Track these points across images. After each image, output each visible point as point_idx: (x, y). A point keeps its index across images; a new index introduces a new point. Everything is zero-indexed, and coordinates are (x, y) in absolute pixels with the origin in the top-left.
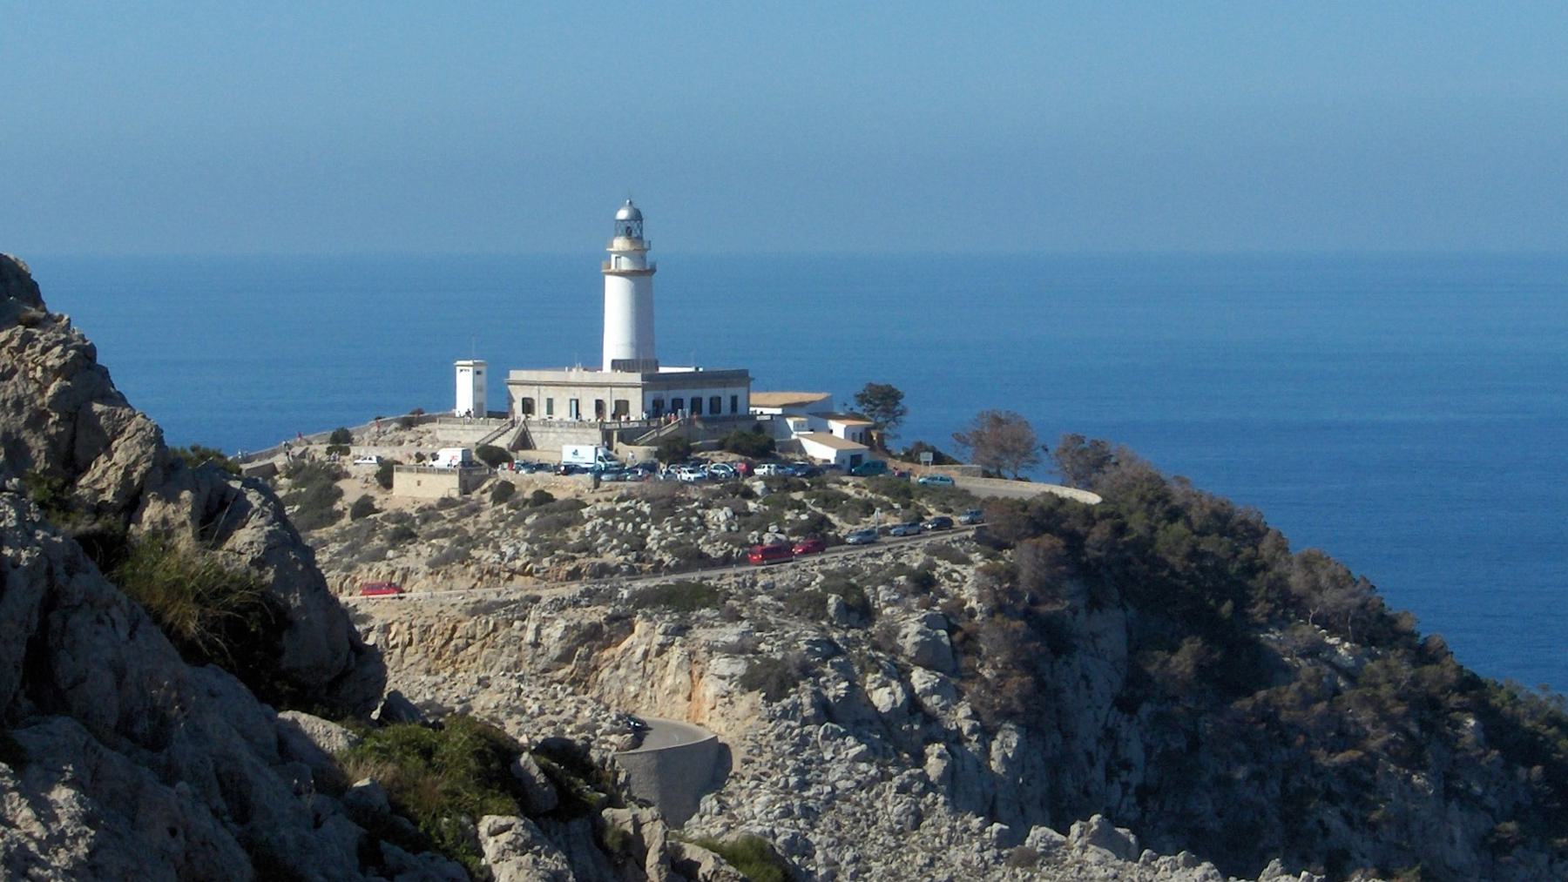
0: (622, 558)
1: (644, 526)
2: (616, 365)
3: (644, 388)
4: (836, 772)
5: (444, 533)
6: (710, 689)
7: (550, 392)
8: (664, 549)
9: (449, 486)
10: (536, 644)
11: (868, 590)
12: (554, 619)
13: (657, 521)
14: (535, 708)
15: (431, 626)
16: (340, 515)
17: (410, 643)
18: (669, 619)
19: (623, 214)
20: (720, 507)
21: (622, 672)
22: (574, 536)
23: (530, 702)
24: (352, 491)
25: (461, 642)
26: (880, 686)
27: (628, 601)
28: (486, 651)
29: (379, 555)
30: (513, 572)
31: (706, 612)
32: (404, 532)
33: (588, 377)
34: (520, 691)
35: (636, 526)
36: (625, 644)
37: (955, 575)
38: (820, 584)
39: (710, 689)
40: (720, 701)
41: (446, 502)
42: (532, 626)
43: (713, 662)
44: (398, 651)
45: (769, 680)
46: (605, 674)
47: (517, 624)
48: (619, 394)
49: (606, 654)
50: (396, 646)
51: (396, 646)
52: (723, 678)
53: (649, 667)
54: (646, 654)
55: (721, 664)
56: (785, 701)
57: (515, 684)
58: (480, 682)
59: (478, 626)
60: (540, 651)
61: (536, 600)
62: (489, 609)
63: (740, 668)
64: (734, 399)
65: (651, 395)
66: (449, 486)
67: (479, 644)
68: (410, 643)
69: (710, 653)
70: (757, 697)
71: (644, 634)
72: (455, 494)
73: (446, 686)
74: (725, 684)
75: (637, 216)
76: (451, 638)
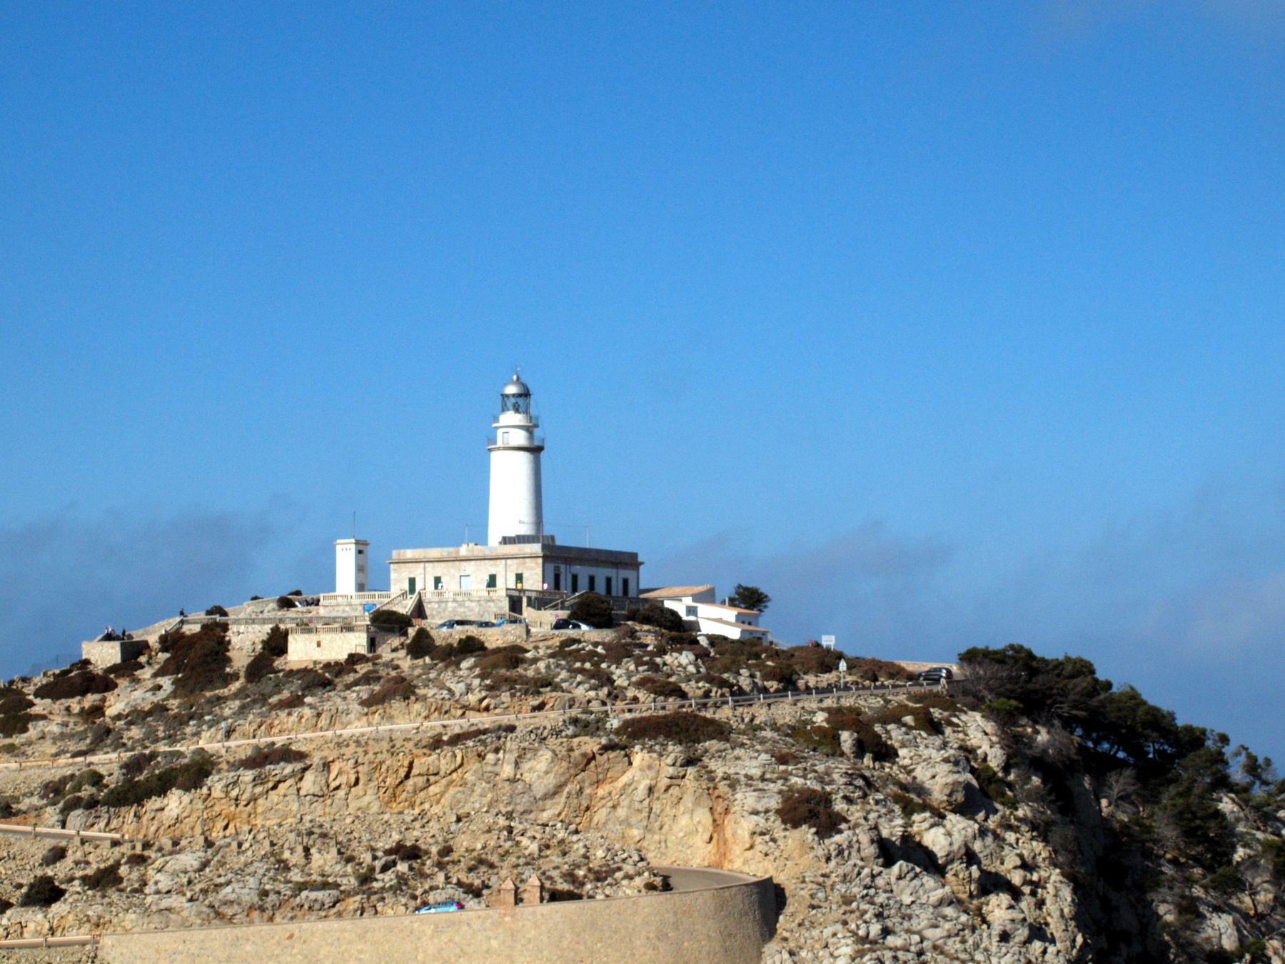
0: (592, 694)
1: (604, 666)
2: (506, 541)
3: (546, 559)
4: (922, 919)
6: (741, 827)
7: (439, 570)
9: (357, 642)
10: (512, 781)
12: (536, 750)
14: (534, 848)
15: (381, 763)
17: (357, 782)
18: (675, 751)
19: (512, 390)
20: (680, 651)
21: (622, 812)
23: (525, 841)
25: (421, 781)
26: (932, 826)
27: (617, 732)
28: (452, 791)
30: (466, 708)
31: (713, 745)
32: (320, 679)
33: (479, 550)
34: (510, 830)
35: (596, 665)
36: (625, 779)
37: (955, 720)
38: (827, 720)
39: (741, 827)
40: (758, 839)
41: (354, 659)
42: (511, 757)
43: (739, 796)
44: (341, 793)
45: (810, 812)
46: (601, 815)
47: (491, 757)
49: (601, 792)
50: (337, 788)
51: (337, 788)
52: (756, 813)
53: (657, 807)
54: (651, 790)
55: (746, 798)
56: (837, 838)
57: (502, 821)
58: (459, 820)
59: (443, 760)
60: (520, 786)
61: (511, 729)
62: (456, 740)
63: (774, 803)
64: (626, 582)
65: (550, 567)
66: (357, 642)
67: (444, 782)
68: (357, 782)
71: (645, 766)
72: (363, 650)
73: (417, 824)
74: (760, 819)
75: (525, 394)
76: (407, 776)
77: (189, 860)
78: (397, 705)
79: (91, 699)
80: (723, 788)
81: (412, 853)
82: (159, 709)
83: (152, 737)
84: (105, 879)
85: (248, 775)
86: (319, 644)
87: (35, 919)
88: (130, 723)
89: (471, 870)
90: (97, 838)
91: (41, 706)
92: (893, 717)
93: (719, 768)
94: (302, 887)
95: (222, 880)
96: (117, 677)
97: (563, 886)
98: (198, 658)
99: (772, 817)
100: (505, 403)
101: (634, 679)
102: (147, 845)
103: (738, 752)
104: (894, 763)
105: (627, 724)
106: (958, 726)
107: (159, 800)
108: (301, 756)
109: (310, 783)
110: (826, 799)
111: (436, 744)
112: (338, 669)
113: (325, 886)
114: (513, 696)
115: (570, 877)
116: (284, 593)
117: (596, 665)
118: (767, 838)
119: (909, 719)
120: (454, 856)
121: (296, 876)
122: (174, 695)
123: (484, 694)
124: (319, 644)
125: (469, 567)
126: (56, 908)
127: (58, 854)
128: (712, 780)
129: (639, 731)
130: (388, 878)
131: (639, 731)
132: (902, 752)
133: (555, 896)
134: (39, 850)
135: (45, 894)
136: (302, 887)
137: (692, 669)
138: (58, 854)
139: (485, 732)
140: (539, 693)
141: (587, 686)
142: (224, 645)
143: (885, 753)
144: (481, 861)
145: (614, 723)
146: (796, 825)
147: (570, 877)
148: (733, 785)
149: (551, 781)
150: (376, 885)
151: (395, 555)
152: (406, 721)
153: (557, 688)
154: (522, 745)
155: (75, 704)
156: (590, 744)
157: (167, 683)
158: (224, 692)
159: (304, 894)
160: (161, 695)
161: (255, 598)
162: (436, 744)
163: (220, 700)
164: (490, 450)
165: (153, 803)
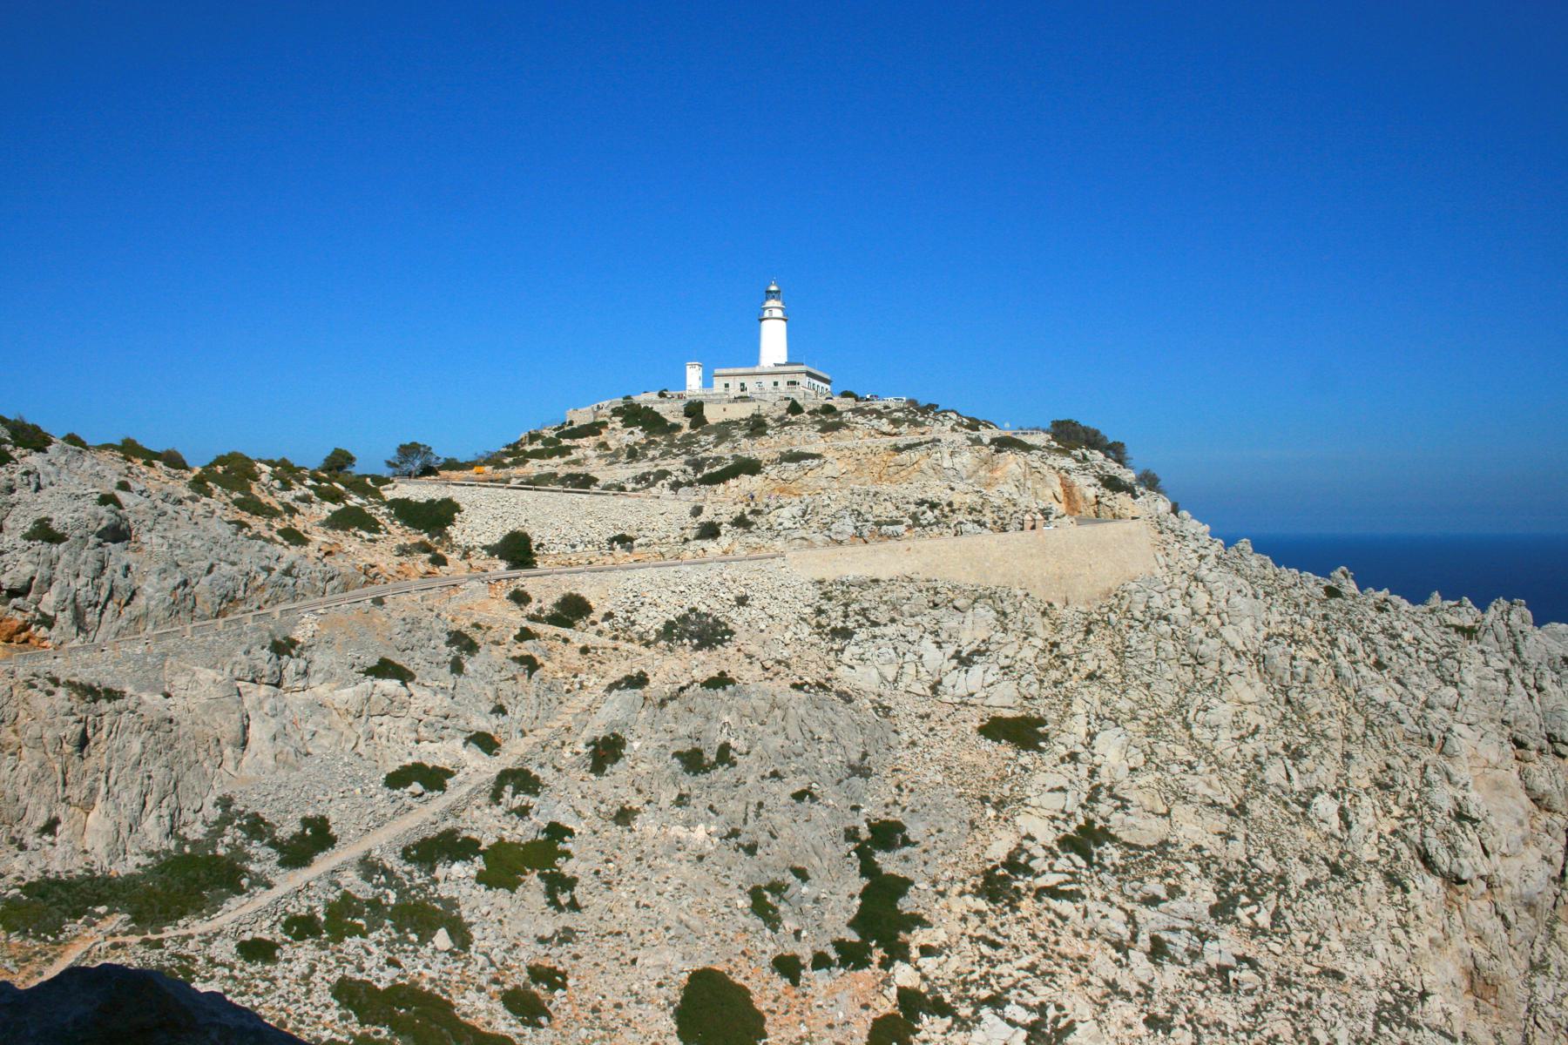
7: (743, 379)
48: (790, 378)
81: (933, 506)
84: (741, 522)
87: (709, 545)
100: (770, 295)
108: (818, 456)
111: (898, 450)
127: (697, 511)
135: (710, 531)
149: (971, 468)
151: (717, 371)
165: (732, 482)
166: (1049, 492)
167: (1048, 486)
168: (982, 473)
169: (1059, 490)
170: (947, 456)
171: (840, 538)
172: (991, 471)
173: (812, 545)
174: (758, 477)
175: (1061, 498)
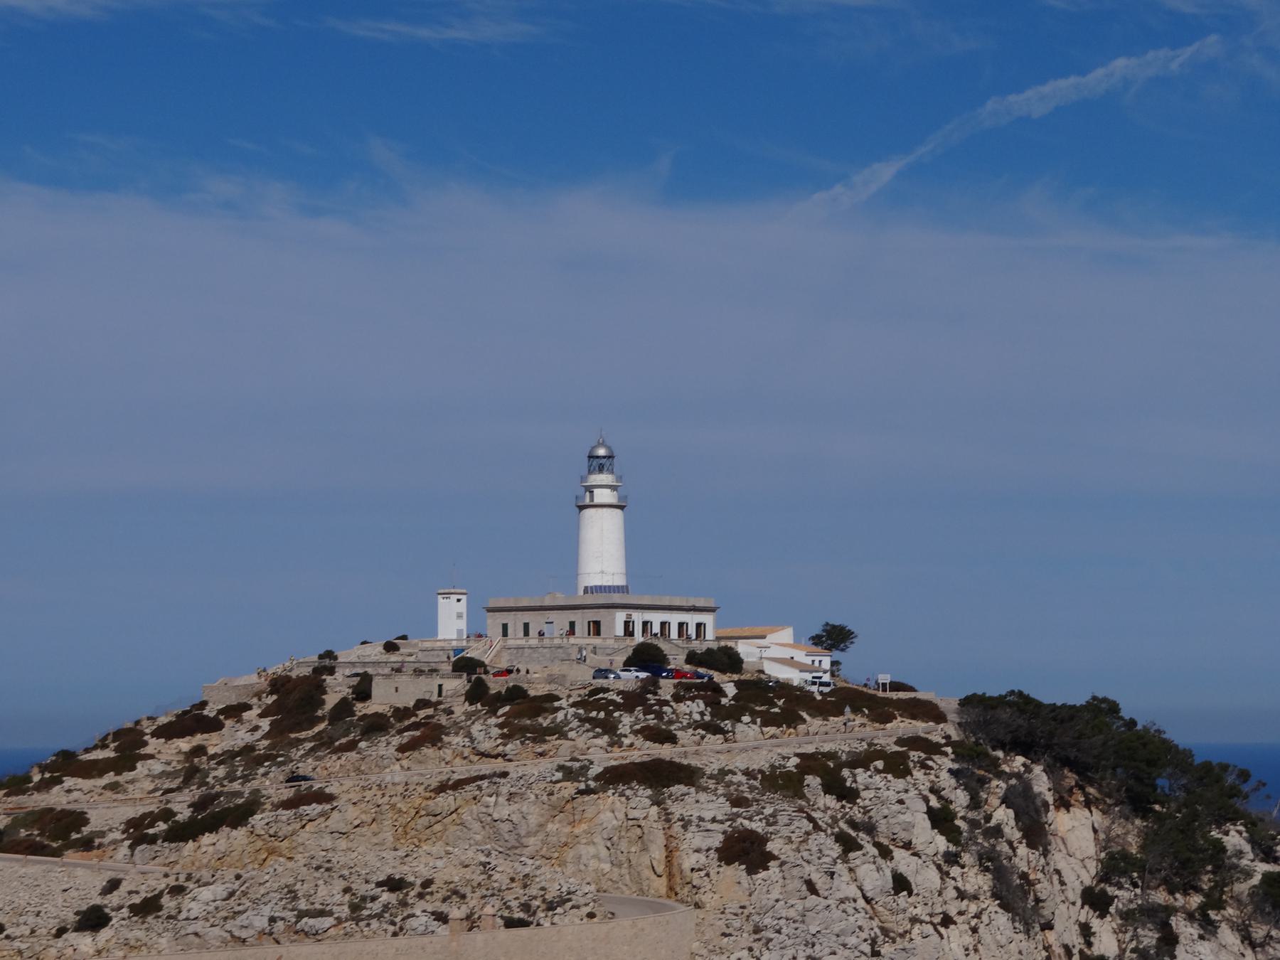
1: (616, 714)
5: (415, 726)
8: (636, 733)
11: (846, 772)
13: (630, 710)
16: (321, 719)
20: (692, 699)
22: (545, 721)
24: (331, 700)
27: (597, 778)
29: (352, 746)
31: (678, 789)
32: (376, 726)
35: (609, 714)
37: (930, 763)
38: (797, 766)
43: (689, 835)
61: (505, 775)
62: (458, 785)
63: (717, 840)
69: (685, 827)
70: (737, 871)
74: (702, 858)
77: (219, 890)
78: (428, 751)
79: (198, 739)
80: (677, 827)
81: (394, 884)
82: (249, 749)
83: (231, 777)
84: (147, 907)
85: (285, 814)
86: (397, 690)
87: (85, 942)
88: (219, 763)
89: (444, 900)
90: (145, 873)
91: (153, 745)
92: (861, 761)
93: (677, 810)
94: (301, 915)
95: (241, 908)
96: (226, 718)
97: (522, 915)
98: (295, 701)
99: (713, 854)
101: (638, 727)
102: (189, 878)
103: (703, 797)
104: (855, 803)
105: (607, 770)
106: (931, 768)
107: (213, 835)
108: (330, 798)
109: (335, 821)
110: (762, 840)
111: (442, 788)
112: (402, 713)
113: (322, 913)
114: (522, 743)
115: (526, 907)
116: (391, 638)
117: (609, 714)
118: (702, 873)
119: (880, 764)
120: (433, 888)
121: (303, 905)
122: (265, 737)
123: (499, 741)
124: (397, 690)
125: (552, 616)
126: (105, 934)
127: (113, 885)
128: (668, 820)
129: (615, 777)
130: (376, 907)
131: (615, 777)
132: (863, 794)
133: (510, 923)
134: (101, 882)
135: (93, 920)
136: (301, 915)
137: (697, 717)
138: (113, 885)
139: (482, 778)
140: (545, 741)
141: (591, 734)
142: (321, 689)
143: (848, 795)
144: (455, 892)
145: (595, 770)
146: (729, 863)
147: (526, 907)
148: (686, 824)
150: (365, 913)
152: (433, 765)
153: (563, 736)
154: (513, 790)
155: (185, 744)
156: (569, 788)
157: (265, 724)
158: (303, 735)
159: (305, 919)
160: (259, 734)
161: (363, 643)
162: (442, 788)
163: (300, 742)
164: (582, 508)
165: (207, 839)
166: (646, 860)
167: (645, 849)
168: (550, 827)
169: (658, 854)
170: (502, 800)
171: (244, 934)
172: (572, 823)
173: (205, 947)
174: (240, 834)
175: (660, 868)
